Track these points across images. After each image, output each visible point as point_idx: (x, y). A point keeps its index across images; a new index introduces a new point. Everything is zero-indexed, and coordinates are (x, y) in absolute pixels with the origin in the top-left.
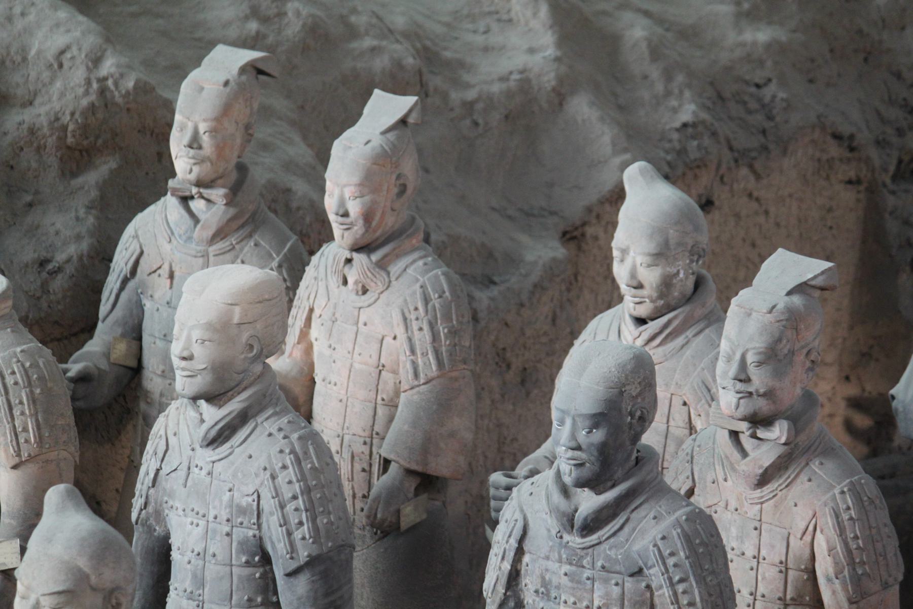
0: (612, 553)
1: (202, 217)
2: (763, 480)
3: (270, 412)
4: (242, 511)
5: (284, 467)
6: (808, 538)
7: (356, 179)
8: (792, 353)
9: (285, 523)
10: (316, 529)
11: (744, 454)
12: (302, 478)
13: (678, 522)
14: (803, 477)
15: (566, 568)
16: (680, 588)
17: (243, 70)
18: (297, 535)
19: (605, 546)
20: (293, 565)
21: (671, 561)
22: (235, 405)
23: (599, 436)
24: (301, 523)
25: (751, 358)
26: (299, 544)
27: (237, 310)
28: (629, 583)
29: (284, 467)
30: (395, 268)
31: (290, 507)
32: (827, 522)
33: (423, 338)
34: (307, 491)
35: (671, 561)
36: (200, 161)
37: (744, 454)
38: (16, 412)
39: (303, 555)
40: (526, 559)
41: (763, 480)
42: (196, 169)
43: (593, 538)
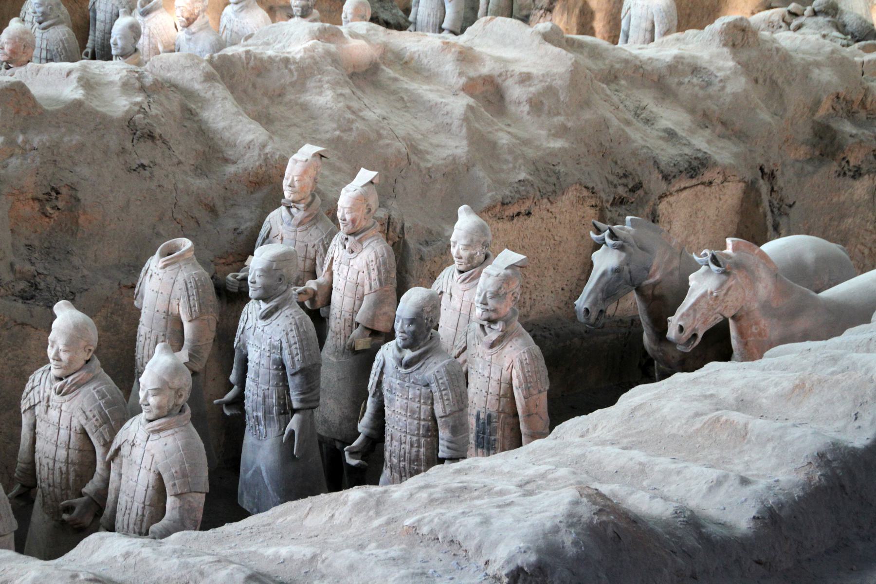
0: (417, 377)
1: (296, 215)
2: (492, 346)
3: (288, 306)
4: (274, 347)
5: (292, 330)
6: (509, 370)
7: (349, 206)
8: (506, 293)
9: (291, 353)
10: (303, 357)
11: (486, 334)
12: (299, 335)
13: (444, 366)
14: (508, 346)
15: (398, 381)
16: (444, 393)
17: (314, 155)
18: (296, 359)
19: (414, 373)
20: (294, 371)
21: (440, 381)
22: (273, 303)
23: (412, 328)
24: (297, 354)
25: (488, 295)
26: (296, 363)
27: (275, 264)
28: (424, 390)
29: (292, 330)
30: (365, 244)
31: (294, 347)
32: (517, 364)
33: (374, 275)
34: (301, 341)
35: (440, 381)
36: (294, 192)
37: (486, 334)
38: (191, 298)
39: (298, 367)
40: (384, 376)
41: (492, 346)
42: (292, 196)
43: (409, 370)
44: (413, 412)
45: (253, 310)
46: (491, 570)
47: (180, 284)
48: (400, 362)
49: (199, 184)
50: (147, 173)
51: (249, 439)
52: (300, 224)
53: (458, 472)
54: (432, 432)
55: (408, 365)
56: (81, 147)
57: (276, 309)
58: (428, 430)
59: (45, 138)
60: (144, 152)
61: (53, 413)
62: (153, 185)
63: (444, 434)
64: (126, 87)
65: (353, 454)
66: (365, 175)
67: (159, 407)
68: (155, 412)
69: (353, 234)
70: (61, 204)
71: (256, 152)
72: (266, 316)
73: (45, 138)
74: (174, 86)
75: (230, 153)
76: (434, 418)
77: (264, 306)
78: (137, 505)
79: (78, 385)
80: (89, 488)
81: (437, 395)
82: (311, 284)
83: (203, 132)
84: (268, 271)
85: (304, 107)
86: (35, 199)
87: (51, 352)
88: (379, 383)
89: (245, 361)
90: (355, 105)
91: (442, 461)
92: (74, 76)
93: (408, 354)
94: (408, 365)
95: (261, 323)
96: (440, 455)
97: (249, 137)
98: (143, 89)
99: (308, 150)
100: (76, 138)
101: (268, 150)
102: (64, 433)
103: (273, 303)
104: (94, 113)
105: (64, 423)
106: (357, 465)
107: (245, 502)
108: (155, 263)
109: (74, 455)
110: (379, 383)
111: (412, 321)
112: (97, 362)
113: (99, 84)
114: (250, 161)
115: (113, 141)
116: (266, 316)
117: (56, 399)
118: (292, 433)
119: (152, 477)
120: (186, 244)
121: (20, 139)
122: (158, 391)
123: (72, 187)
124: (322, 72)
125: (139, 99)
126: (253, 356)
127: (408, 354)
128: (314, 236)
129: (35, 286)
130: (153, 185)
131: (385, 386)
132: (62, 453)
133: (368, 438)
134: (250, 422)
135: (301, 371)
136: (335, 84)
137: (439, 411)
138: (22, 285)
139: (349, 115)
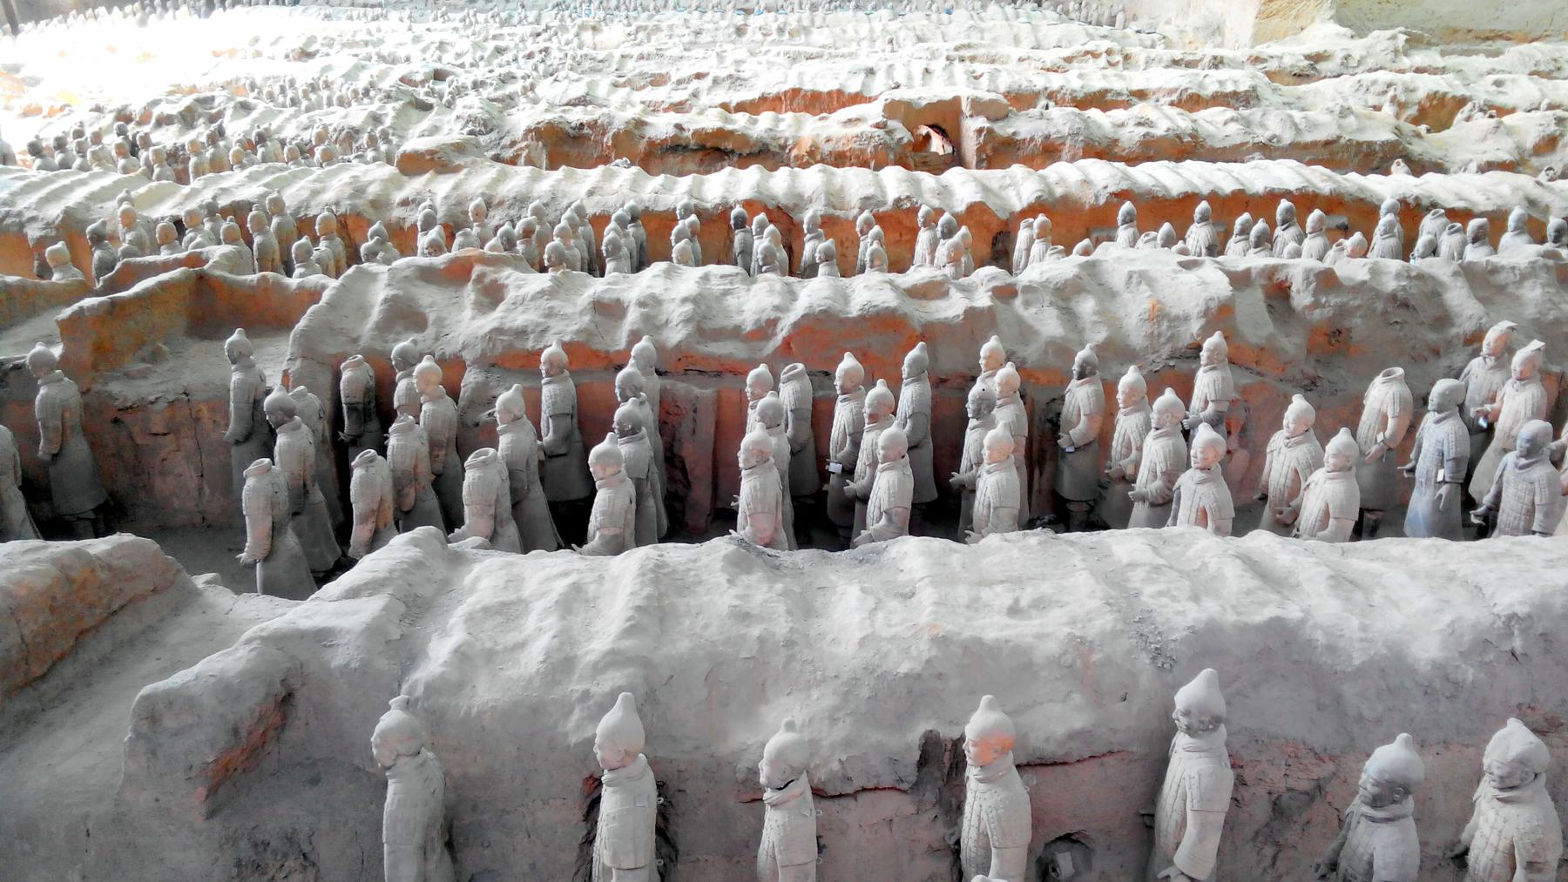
22: (1443, 415)
33: (1529, 407)
39: (1452, 456)
44: (1519, 498)
45: (1430, 418)
46: (1495, 610)
47: (1390, 395)
48: (1516, 465)
49: (1432, 337)
50: (1398, 327)
51: (1415, 494)
52: (1491, 368)
53: (1513, 543)
54: (1531, 512)
55: (1522, 468)
56: (1358, 307)
57: (1444, 418)
58: (1528, 511)
59: (1338, 300)
60: (1398, 315)
61: (1282, 457)
62: (1401, 334)
63: (1538, 516)
64: (1398, 276)
65: (1476, 516)
66: (1537, 344)
67: (1335, 465)
68: (1332, 468)
69: (1520, 380)
70: (1340, 339)
71: (1474, 321)
72: (1438, 422)
73: (1338, 300)
74: (1432, 278)
75: (1457, 321)
76: (1533, 504)
77: (1438, 416)
78: (1313, 519)
79: (1298, 443)
80: (1293, 503)
81: (1537, 490)
82: (1488, 407)
83: (1442, 306)
84: (1443, 395)
85: (1518, 298)
86: (1326, 335)
87: (1285, 422)
88: (1501, 476)
89: (1420, 447)
90: (1556, 299)
91: (1534, 533)
92: (1366, 268)
93: (1523, 461)
94: (1522, 468)
95: (1434, 426)
96: (1534, 528)
97: (1471, 313)
98: (1409, 277)
99: (1505, 325)
100: (1357, 302)
101: (1483, 321)
102: (1285, 468)
103: (1443, 415)
104: (1372, 289)
105: (1286, 464)
106: (110, 553)
107: (1407, 529)
108: (1379, 379)
109: (1289, 482)
110: (1501, 476)
111: (1528, 441)
112: (1312, 431)
113: (1382, 272)
114: (1465, 326)
115: (1380, 306)
116: (1438, 422)
117: (1284, 449)
118: (1441, 496)
119: (1323, 506)
120: (1399, 371)
121: (1324, 300)
122: (1335, 456)
123: (1349, 330)
124: (1536, 277)
125: (1403, 283)
126: (1425, 446)
127: (1523, 461)
128: (1497, 377)
129: (1314, 383)
130: (1401, 334)
131: (1505, 479)
132: (1283, 480)
133: (1489, 509)
134: (1417, 484)
135: (1454, 459)
136: (1543, 286)
137: (1537, 501)
138: (1307, 382)
139: (1549, 305)
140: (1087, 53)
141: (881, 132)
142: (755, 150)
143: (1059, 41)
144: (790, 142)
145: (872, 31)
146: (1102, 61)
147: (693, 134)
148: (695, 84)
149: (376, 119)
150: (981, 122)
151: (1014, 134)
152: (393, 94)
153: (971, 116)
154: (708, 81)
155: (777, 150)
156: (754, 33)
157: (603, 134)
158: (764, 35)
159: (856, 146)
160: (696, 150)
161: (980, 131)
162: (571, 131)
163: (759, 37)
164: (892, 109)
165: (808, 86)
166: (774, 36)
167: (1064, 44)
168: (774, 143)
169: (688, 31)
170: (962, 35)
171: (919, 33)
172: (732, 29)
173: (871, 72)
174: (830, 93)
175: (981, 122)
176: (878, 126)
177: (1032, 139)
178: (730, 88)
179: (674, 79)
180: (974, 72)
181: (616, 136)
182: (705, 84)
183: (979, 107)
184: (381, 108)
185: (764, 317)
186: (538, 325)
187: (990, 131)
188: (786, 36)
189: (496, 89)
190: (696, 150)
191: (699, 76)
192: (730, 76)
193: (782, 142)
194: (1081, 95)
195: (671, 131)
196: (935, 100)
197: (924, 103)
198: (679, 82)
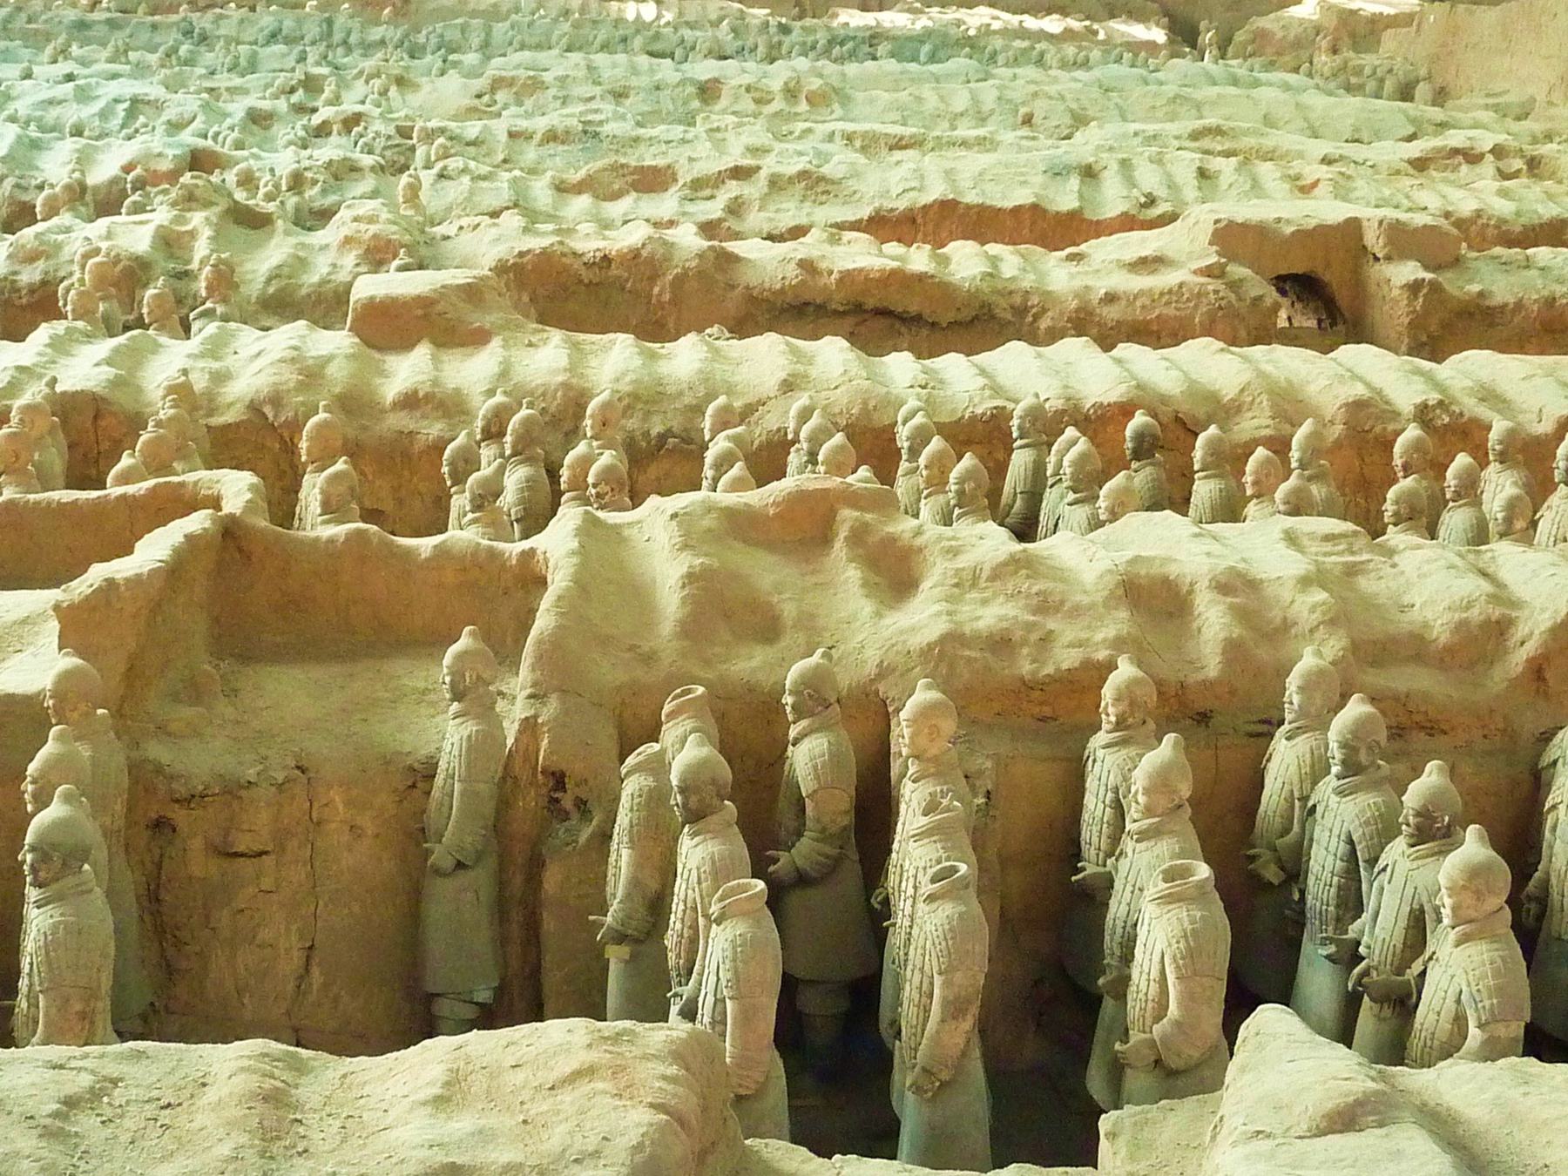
140: (1455, 152)
141: (1212, 285)
142: (966, 315)
143: (1357, 130)
144: (1035, 300)
145: (975, 100)
146: (1488, 166)
147: (840, 281)
148: (733, 189)
149: (169, 242)
150: (1408, 271)
151: (1481, 294)
152: (198, 193)
153: (1388, 258)
154: (760, 183)
155: (1009, 317)
156: (737, 98)
157: (653, 279)
158: (758, 101)
159: (1170, 311)
160: (844, 313)
161: (1414, 287)
162: (583, 271)
163: (747, 104)
164: (1230, 237)
165: (971, 198)
166: (778, 105)
167: (1365, 136)
168: (1003, 303)
169: (597, 90)
170: (1160, 114)
171: (1074, 106)
172: (691, 89)
173: (1089, 173)
174: (1017, 210)
175: (1408, 271)
176: (1208, 272)
177: (1519, 305)
178: (804, 199)
179: (685, 176)
180: (1297, 178)
181: (680, 280)
182: (751, 191)
183: (1403, 240)
184: (179, 220)
185: (1475, 614)
186: (1029, 627)
187: (1435, 287)
188: (803, 106)
189: (324, 192)
190: (844, 313)
191: (739, 173)
192: (804, 175)
193: (1018, 300)
194: (1518, 229)
195: (792, 273)
196: (1312, 223)
197: (1289, 230)
198: (697, 184)
